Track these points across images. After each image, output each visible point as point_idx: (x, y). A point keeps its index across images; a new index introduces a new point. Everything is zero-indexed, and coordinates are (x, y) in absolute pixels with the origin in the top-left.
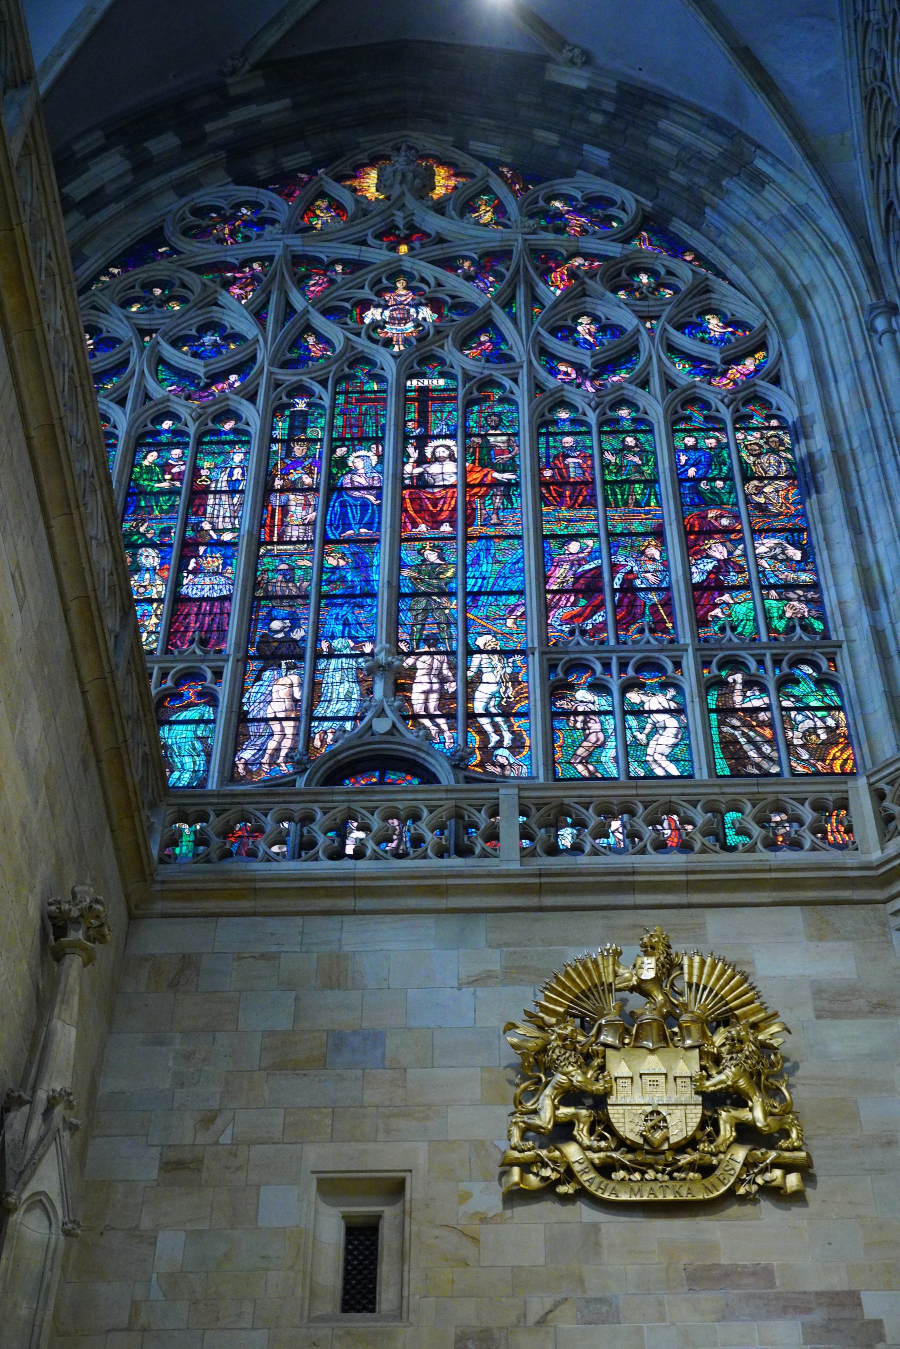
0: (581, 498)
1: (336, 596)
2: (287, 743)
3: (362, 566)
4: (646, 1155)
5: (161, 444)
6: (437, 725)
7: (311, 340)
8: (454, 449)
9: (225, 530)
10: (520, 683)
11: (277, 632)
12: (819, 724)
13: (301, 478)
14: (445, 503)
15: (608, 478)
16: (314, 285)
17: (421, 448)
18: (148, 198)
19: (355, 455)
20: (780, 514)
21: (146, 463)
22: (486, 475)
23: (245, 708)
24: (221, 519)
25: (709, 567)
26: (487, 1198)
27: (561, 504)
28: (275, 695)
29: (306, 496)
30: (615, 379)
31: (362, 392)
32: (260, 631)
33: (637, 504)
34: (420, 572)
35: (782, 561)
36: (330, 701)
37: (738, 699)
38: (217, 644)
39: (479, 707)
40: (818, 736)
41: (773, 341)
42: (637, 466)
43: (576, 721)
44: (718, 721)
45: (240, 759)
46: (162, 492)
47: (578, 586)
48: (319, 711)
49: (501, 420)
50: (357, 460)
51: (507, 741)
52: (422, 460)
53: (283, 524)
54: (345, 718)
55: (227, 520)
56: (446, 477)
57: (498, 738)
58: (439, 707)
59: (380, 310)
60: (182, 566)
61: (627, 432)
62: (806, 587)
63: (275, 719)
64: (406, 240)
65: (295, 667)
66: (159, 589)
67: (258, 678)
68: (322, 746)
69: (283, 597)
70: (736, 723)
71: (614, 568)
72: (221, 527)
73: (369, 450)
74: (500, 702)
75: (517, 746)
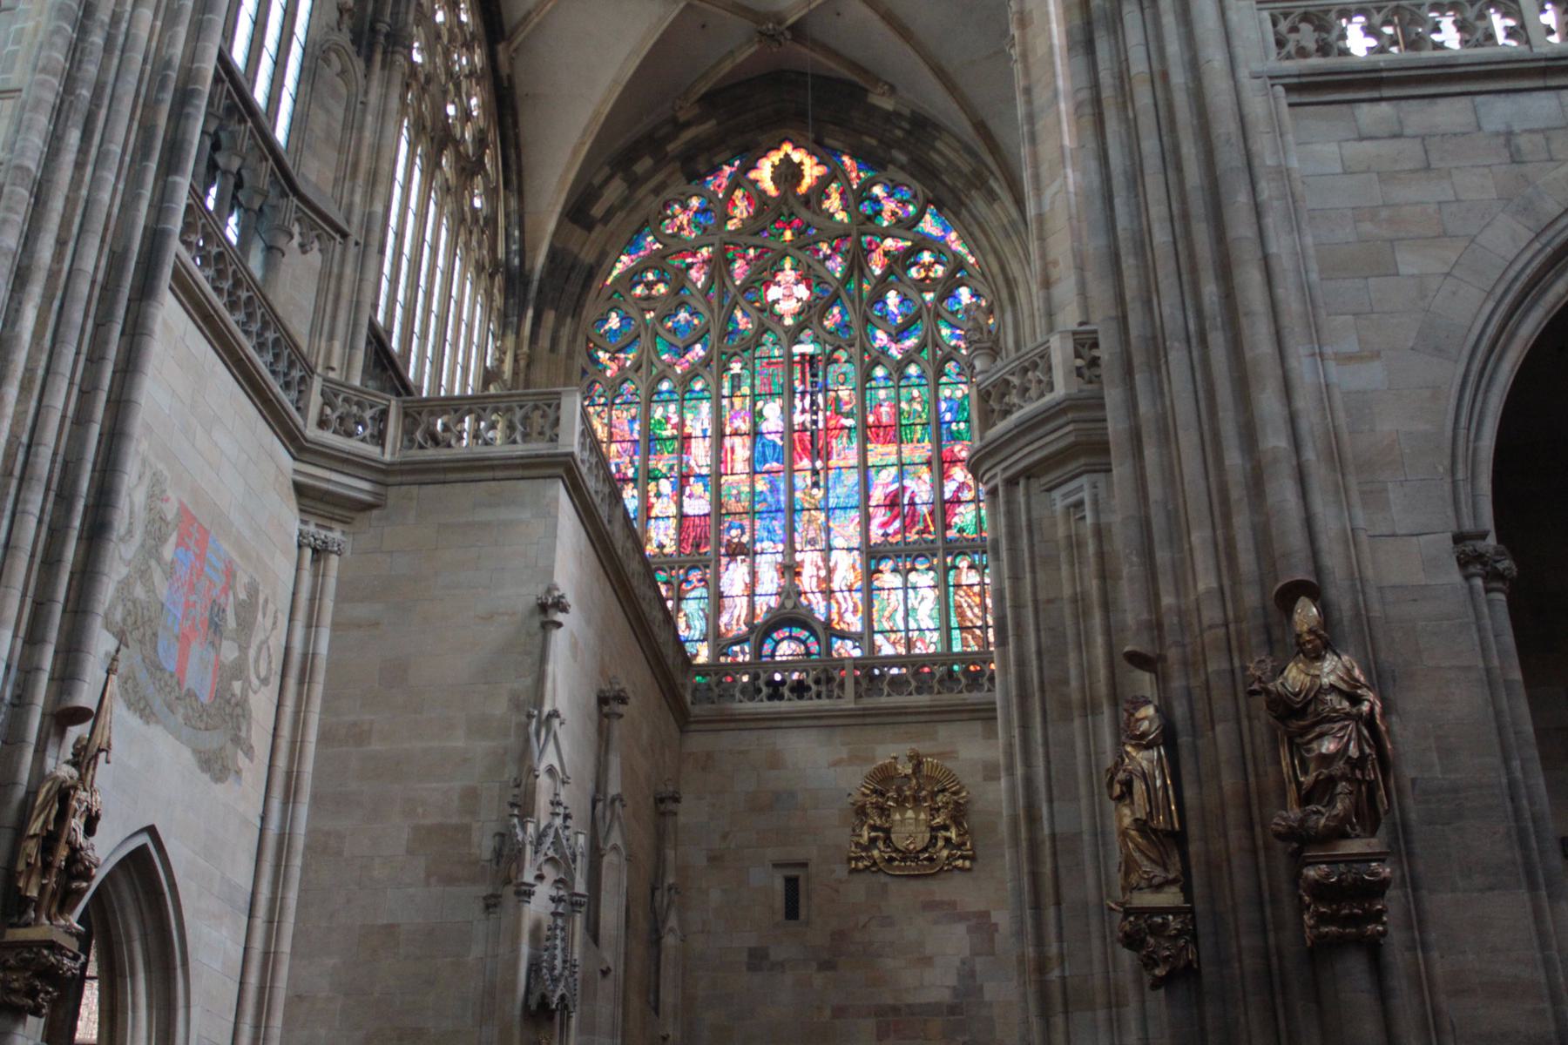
2: (744, 612)
4: (905, 855)
7: (739, 314)
15: (904, 422)
18: (639, 202)
26: (841, 871)
32: (726, 538)
39: (835, 586)
41: (997, 312)
46: (668, 439)
60: (682, 493)
64: (789, 225)
66: (673, 510)
71: (904, 489)
75: (855, 612)
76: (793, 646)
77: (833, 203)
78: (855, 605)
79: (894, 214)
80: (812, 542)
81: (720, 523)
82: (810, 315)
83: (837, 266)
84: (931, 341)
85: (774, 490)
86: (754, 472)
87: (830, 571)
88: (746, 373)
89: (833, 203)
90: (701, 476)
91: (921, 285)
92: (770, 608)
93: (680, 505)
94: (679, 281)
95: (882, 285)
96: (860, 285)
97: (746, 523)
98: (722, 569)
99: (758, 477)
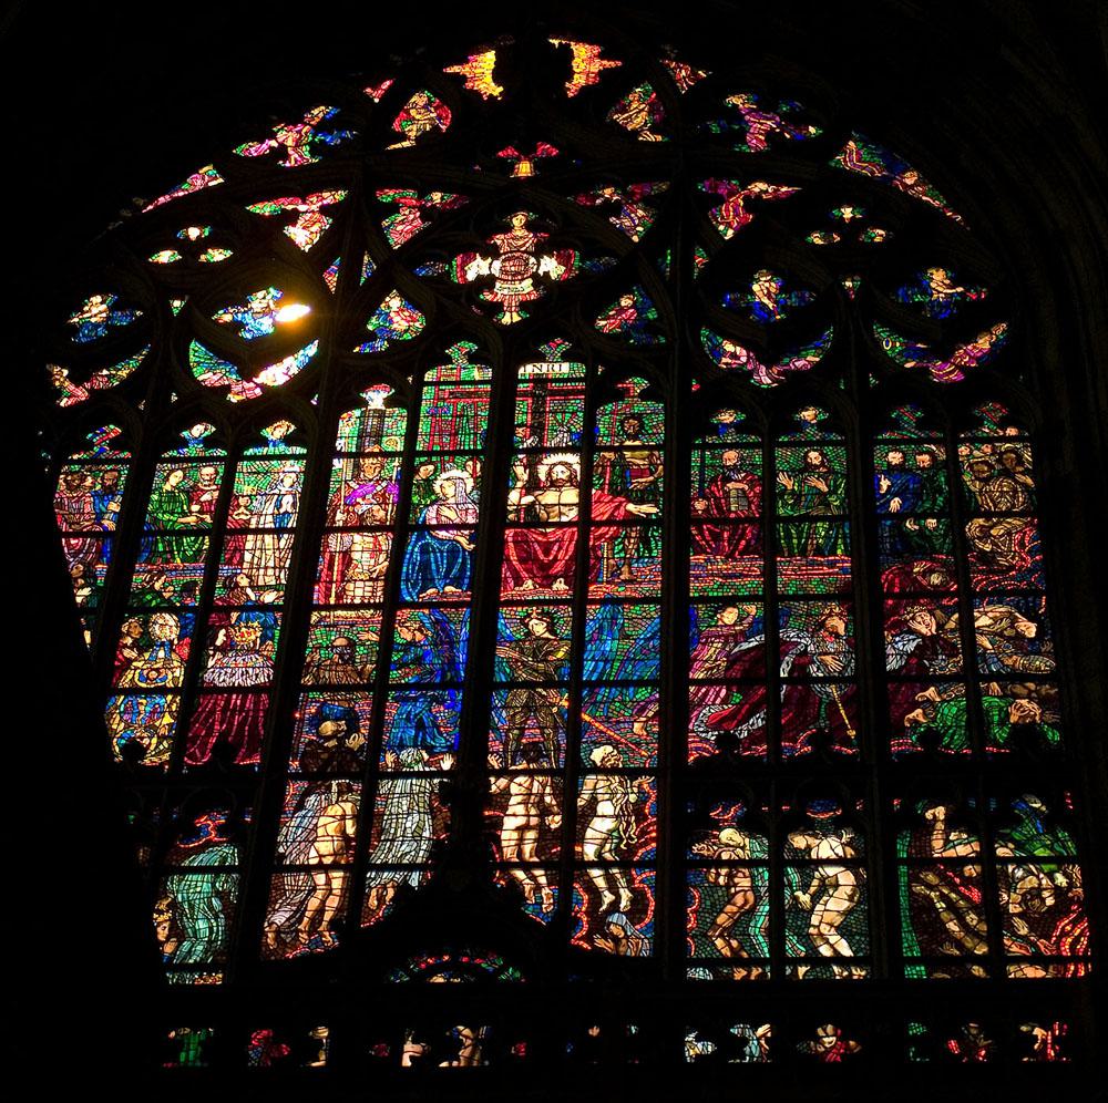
0: (743, 542)
1: (408, 686)
2: (333, 902)
5: (189, 460)
6: (533, 878)
9: (267, 587)
10: (646, 818)
11: (328, 738)
14: (560, 548)
16: (402, 222)
17: (531, 467)
19: (444, 476)
20: (1012, 568)
21: (167, 487)
22: (617, 508)
23: (281, 850)
24: (262, 571)
25: (911, 647)
27: (717, 552)
28: (321, 831)
29: (376, 538)
30: (799, 364)
33: (819, 551)
34: (522, 652)
36: (393, 840)
37: (938, 844)
38: (250, 757)
40: (1043, 900)
42: (820, 493)
43: (718, 875)
44: (909, 875)
45: (270, 925)
48: (378, 857)
49: (642, 426)
50: (446, 484)
51: (624, 904)
52: (533, 485)
54: (412, 867)
55: (270, 572)
56: (564, 509)
58: (537, 852)
61: (811, 444)
62: (1040, 679)
65: (350, 789)
67: (300, 806)
68: (379, 907)
70: (931, 878)
72: (261, 583)
73: (464, 468)
74: (618, 845)
75: (635, 913)
78: (638, 899)
80: (533, 752)
83: (635, 222)
84: (853, 354)
85: (444, 637)
86: (391, 604)
87: (577, 820)
93: (195, 665)
95: (737, 263)
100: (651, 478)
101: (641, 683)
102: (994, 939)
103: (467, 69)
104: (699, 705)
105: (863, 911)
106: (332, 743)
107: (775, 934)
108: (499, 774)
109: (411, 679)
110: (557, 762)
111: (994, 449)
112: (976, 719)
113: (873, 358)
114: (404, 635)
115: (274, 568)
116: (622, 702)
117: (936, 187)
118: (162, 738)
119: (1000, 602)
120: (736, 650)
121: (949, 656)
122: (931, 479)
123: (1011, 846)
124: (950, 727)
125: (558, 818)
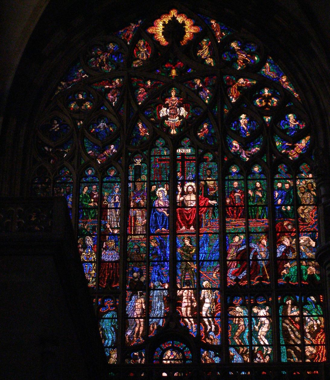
0: (240, 214)
1: (155, 261)
2: (142, 329)
3: (162, 246)
6: (190, 321)
8: (194, 187)
10: (217, 304)
11: (136, 278)
12: (315, 323)
13: (140, 202)
14: (191, 216)
15: (250, 204)
19: (159, 190)
20: (309, 223)
22: (206, 202)
24: (113, 223)
25: (283, 250)
27: (233, 217)
30: (253, 150)
31: (160, 156)
32: (130, 278)
35: (308, 247)
36: (155, 310)
37: (289, 311)
38: (116, 284)
39: (204, 313)
43: (236, 321)
46: (92, 208)
47: (239, 258)
50: (160, 192)
51: (213, 329)
52: (183, 194)
53: (135, 226)
54: (160, 318)
55: (115, 223)
57: (210, 327)
58: (191, 314)
59: (166, 109)
61: (257, 179)
63: (137, 318)
66: (94, 257)
67: (131, 300)
68: (153, 330)
69: (137, 262)
70: (288, 322)
72: (113, 227)
73: (164, 188)
74: (211, 312)
75: (216, 332)
76: (175, 354)
77: (204, 52)
79: (245, 61)
81: (126, 267)
82: (188, 127)
83: (206, 96)
84: (269, 148)
85: (162, 246)
86: (148, 234)
87: (201, 303)
88: (145, 165)
89: (204, 52)
90: (114, 234)
91: (262, 112)
92: (159, 327)
93: (99, 254)
94: (100, 99)
95: (237, 110)
96: (222, 109)
97: (144, 268)
98: (127, 299)
99: (152, 237)
100: (215, 191)
101: (214, 261)
102: (302, 340)
103: (154, 30)
104: (230, 268)
105: (271, 331)
106: (137, 280)
107: (250, 338)
108: (180, 289)
109: (156, 259)
110: (194, 286)
111: (306, 182)
112: (299, 271)
113: (273, 149)
114: (153, 244)
115: (116, 221)
116: (210, 267)
117: (291, 83)
118: (93, 278)
119: (306, 235)
120: (238, 250)
121: (293, 253)
122: (289, 193)
123: (307, 312)
124: (293, 275)
125: (195, 303)
